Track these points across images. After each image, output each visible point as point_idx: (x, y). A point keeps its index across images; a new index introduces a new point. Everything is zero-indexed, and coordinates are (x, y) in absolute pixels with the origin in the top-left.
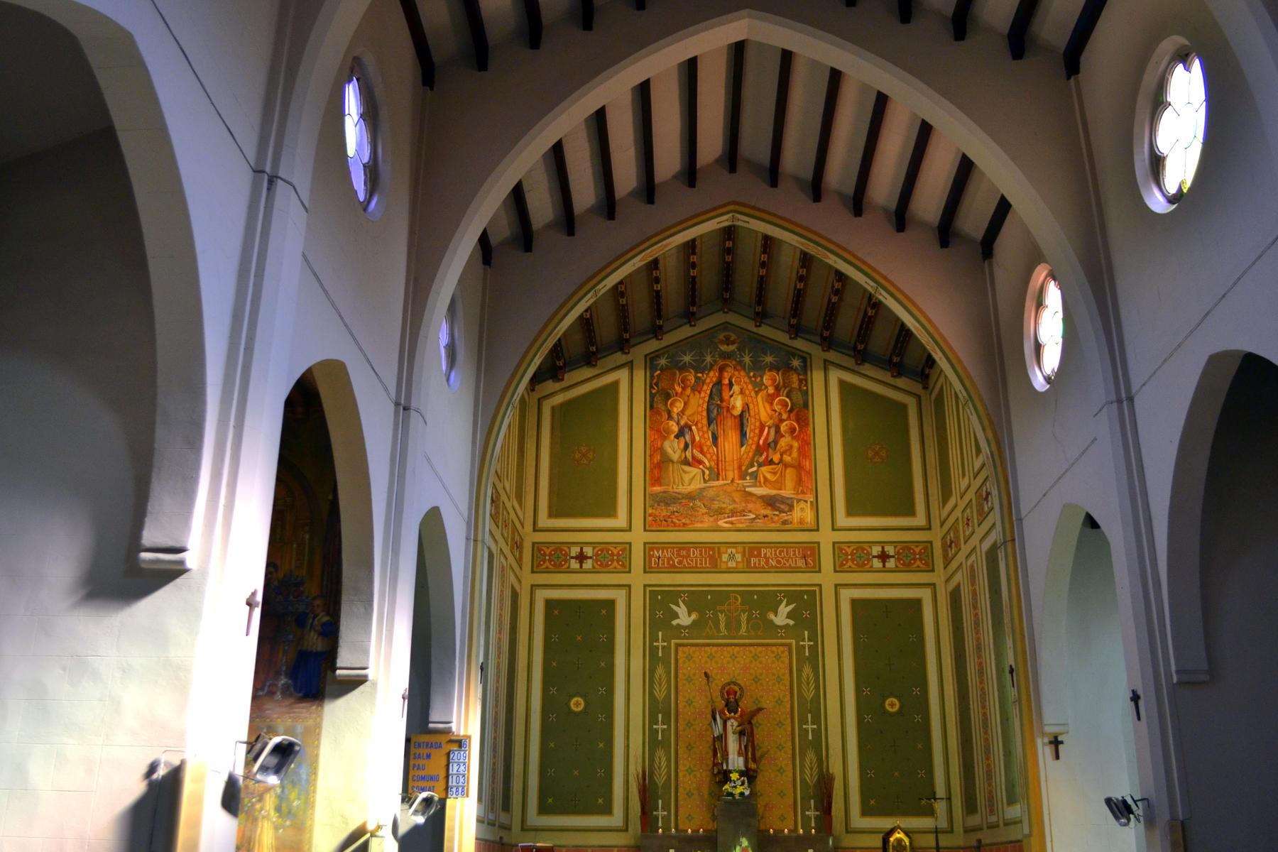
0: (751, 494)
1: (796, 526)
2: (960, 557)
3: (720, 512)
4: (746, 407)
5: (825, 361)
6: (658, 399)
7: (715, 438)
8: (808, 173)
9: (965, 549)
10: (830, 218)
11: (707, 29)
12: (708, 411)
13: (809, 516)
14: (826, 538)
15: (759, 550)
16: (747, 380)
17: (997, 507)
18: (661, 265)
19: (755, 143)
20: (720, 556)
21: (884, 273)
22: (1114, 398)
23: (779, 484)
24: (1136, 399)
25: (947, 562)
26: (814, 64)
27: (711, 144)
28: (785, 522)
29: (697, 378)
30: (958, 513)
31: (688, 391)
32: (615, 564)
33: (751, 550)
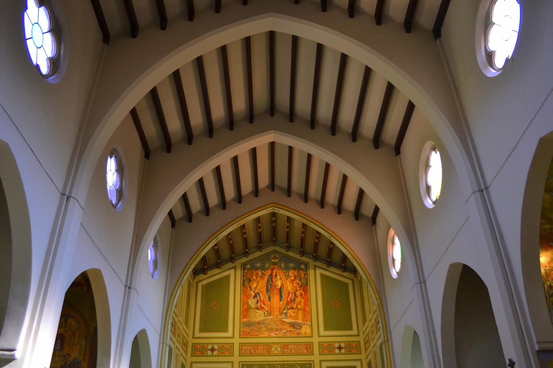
0: (284, 322)
1: (303, 335)
2: (370, 348)
3: (271, 330)
4: (282, 285)
5: (315, 266)
6: (246, 281)
7: (269, 298)
8: (302, 191)
9: (372, 344)
10: (312, 209)
11: (257, 137)
12: (267, 287)
13: (308, 331)
14: (316, 340)
15: (288, 346)
16: (283, 274)
17: (381, 327)
18: (246, 227)
19: (281, 179)
20: (271, 348)
21: (333, 230)
22: (418, 282)
23: (296, 317)
24: (427, 282)
25: (366, 349)
26: (301, 151)
27: (264, 180)
28: (298, 334)
29: (262, 273)
30: (368, 329)
31: (259, 279)
32: (227, 352)
33: (285, 346)
